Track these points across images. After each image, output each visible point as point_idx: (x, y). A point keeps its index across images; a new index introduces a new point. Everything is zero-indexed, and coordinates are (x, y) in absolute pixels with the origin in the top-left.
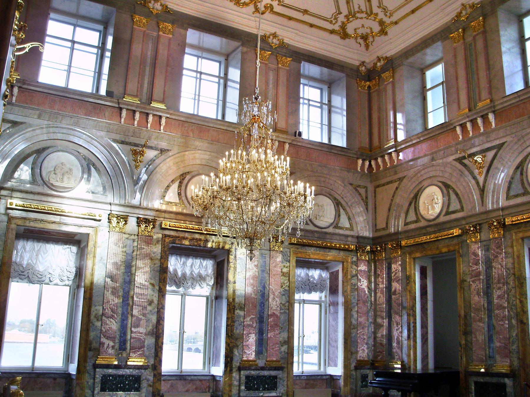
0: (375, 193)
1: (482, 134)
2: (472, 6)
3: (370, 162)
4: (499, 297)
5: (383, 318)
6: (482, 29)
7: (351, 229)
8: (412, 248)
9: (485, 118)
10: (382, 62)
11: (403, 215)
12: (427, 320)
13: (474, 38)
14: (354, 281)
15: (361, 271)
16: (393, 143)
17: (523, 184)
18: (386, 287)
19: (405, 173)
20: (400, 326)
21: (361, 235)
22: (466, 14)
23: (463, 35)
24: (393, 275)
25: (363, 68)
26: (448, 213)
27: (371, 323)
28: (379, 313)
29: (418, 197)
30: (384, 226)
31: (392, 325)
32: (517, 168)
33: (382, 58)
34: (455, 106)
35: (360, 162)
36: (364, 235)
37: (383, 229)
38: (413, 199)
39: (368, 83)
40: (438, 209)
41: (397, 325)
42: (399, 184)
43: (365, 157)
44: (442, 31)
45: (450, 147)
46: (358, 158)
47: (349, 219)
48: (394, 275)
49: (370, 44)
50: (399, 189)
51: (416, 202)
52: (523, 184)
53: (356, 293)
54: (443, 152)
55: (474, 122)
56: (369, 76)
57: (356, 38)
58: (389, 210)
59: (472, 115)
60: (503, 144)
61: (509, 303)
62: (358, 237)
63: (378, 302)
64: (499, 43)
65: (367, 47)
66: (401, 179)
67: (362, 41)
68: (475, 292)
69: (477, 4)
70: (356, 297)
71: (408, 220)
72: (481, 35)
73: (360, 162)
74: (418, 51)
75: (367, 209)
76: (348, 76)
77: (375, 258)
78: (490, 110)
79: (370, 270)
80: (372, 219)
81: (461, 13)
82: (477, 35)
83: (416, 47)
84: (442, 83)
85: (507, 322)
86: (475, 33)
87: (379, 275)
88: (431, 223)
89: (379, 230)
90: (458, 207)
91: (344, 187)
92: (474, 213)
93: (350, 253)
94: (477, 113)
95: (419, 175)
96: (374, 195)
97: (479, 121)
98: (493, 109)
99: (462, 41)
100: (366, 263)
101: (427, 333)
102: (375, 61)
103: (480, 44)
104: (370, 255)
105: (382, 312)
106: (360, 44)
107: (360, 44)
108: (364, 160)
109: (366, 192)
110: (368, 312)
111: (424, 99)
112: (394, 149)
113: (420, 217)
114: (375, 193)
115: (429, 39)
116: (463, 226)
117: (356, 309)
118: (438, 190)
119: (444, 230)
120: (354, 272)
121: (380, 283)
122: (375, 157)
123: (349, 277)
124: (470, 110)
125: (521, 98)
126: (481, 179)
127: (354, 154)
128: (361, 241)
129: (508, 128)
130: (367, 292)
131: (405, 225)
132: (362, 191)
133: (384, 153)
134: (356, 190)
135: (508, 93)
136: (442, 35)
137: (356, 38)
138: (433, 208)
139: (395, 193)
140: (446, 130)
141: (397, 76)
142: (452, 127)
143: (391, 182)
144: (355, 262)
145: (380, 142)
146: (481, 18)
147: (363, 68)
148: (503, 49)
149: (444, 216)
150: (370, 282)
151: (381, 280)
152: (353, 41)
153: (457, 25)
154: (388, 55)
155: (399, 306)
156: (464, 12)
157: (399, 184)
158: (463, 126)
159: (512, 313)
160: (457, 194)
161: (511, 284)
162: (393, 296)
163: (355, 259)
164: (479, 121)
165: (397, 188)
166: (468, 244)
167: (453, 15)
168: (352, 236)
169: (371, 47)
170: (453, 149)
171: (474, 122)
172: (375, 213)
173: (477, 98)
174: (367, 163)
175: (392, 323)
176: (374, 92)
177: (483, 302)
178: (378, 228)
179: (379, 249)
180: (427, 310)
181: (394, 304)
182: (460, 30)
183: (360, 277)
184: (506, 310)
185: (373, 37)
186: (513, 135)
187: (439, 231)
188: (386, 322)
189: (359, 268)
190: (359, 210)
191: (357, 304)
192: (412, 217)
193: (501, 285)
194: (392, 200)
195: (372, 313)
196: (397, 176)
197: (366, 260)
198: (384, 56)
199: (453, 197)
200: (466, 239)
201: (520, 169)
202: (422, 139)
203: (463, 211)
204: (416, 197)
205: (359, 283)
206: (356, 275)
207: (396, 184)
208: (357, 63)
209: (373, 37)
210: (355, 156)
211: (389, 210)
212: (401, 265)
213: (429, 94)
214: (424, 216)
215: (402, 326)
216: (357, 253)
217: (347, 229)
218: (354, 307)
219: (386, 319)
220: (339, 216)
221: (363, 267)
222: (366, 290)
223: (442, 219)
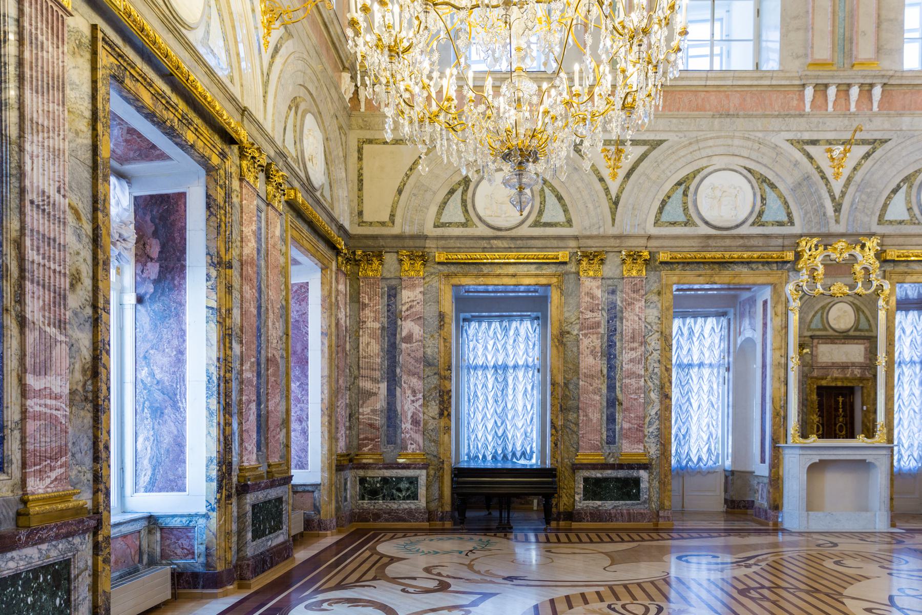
4: (631, 361)
18: (383, 328)
26: (536, 224)
48: (407, 310)
61: (646, 370)
68: (588, 351)
149: (530, 226)
159: (650, 384)
161: (653, 344)
177: (600, 365)
184: (643, 380)
193: (635, 345)
212: (423, 293)
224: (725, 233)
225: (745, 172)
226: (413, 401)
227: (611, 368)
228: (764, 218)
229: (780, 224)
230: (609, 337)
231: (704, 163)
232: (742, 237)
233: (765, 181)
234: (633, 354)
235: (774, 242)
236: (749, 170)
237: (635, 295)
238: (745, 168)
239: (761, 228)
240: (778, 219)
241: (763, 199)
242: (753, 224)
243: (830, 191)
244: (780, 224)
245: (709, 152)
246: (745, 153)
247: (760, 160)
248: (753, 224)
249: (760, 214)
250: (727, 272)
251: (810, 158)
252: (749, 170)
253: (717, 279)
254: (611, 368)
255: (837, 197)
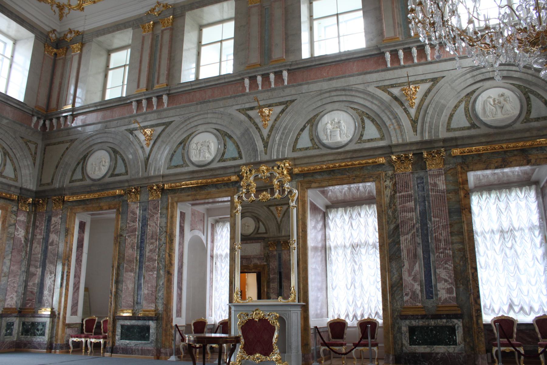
0: (45, 151)
1: (155, 112)
2: (166, 6)
3: (44, 121)
4: (151, 250)
5: (36, 267)
6: (170, 26)
7: (16, 179)
8: (74, 204)
9: (159, 98)
10: (73, 35)
11: (69, 173)
12: (80, 271)
13: (162, 31)
14: (11, 230)
15: (20, 221)
16: (71, 107)
17: (183, 157)
18: (43, 238)
19: (78, 136)
20: (53, 275)
21: (25, 187)
22: (159, 11)
23: (153, 28)
24: (52, 227)
25: (54, 35)
26: (112, 175)
27: (23, 272)
28: (32, 263)
29: (87, 159)
30: (50, 181)
31: (45, 274)
32: (181, 143)
33: (74, 31)
34: (135, 84)
35: (35, 119)
36: (28, 187)
37: (48, 184)
38: (82, 159)
39: (55, 50)
40: (104, 170)
41: (51, 273)
42: (70, 145)
43: (40, 116)
44: (135, 20)
45: (124, 118)
46: (33, 115)
47: (15, 170)
49: (64, 15)
50: (69, 150)
51: (84, 162)
52: (183, 157)
53: (12, 241)
54: (116, 122)
55: (149, 100)
56: (57, 44)
57: (52, 6)
58: (57, 167)
59: (148, 94)
60: (172, 122)
61: (159, 256)
62: (21, 189)
63: (33, 252)
64: (182, 40)
65: (61, 17)
66: (72, 141)
67: (57, 10)
68: (130, 246)
69: (170, 5)
70: (11, 246)
71: (74, 179)
72: (168, 31)
73: (35, 119)
74: (110, 32)
75: (34, 164)
76: (36, 38)
77: (35, 210)
78: (166, 93)
79: (28, 222)
80: (38, 174)
81: (154, 9)
82: (165, 29)
83: (108, 28)
84: (125, 66)
85: (156, 272)
86: (163, 28)
87: (37, 227)
88: (95, 183)
89: (44, 185)
90: (123, 171)
91: (14, 139)
92: (136, 177)
93: (11, 202)
94: (154, 93)
95: (91, 139)
96: (43, 152)
97: (154, 100)
98: (168, 92)
99: (151, 32)
100: (26, 214)
101: (79, 282)
102: (66, 33)
103: (167, 37)
104: (31, 206)
105: (36, 261)
106: (54, 11)
107: (54, 11)
108: (39, 118)
109: (36, 148)
110: (22, 261)
111: (106, 76)
112: (71, 113)
113: (86, 177)
114: (45, 151)
115: (122, 24)
116: (126, 188)
117: (10, 258)
118: (107, 155)
119: (107, 189)
120: (12, 222)
121: (38, 234)
122: (50, 118)
123: (7, 225)
124: (147, 90)
125: (193, 87)
126: (147, 150)
127: (30, 110)
128: (24, 194)
129: (178, 110)
130: (23, 242)
131: (70, 182)
132: (32, 147)
133: (60, 115)
134: (27, 144)
135: (182, 82)
136: (135, 23)
137: (52, 6)
138: (100, 169)
139: (65, 152)
140: (122, 103)
141: (85, 50)
142: (129, 101)
143: (63, 142)
144: (15, 211)
145: (57, 105)
146: (171, 17)
147: (54, 35)
148: (185, 47)
150: (27, 232)
151: (39, 231)
152: (48, 6)
153: (149, 18)
154: (81, 29)
155: (54, 255)
156: (157, 9)
157: (70, 145)
158: (139, 102)
159: (160, 265)
160: (123, 160)
161: (163, 240)
162: (50, 247)
163: (15, 209)
164: (154, 100)
165: (67, 149)
166: (128, 204)
167: (148, 9)
168: (16, 187)
169: (64, 18)
170: (127, 120)
171: (149, 100)
172: (42, 169)
173: (156, 81)
174: (41, 122)
175: (46, 272)
176: (60, 59)
177: (136, 254)
178: (43, 182)
179: (41, 202)
180: (81, 261)
181: (49, 254)
182: (152, 22)
183: (17, 227)
184: (156, 262)
185: (70, 9)
186: (181, 117)
187: (103, 190)
188: (39, 271)
189: (18, 218)
190: (26, 164)
191: (12, 252)
192: (78, 175)
193: (154, 241)
194: (61, 159)
195: (25, 263)
196: (70, 138)
197: (27, 211)
198: (76, 30)
199: (120, 161)
200: (126, 199)
201: (182, 145)
202: (99, 108)
203: (127, 174)
204: (85, 158)
205: (16, 233)
206: (15, 225)
207: (67, 145)
208: (48, 29)
209: (70, 9)
210: (31, 113)
211: (57, 167)
212: (61, 218)
213: (110, 73)
214: (90, 176)
215: (55, 275)
216: (18, 203)
217: (11, 179)
218: (8, 255)
219: (39, 268)
220: (5, 165)
221: (22, 218)
222: (23, 240)
223: (107, 180)
224: (203, 168)
225: (215, 131)
226: (50, 278)
227: (141, 255)
228: (225, 157)
229: (234, 159)
230: (141, 236)
231: (194, 130)
232: (212, 170)
233: (226, 135)
234: (151, 247)
235: (229, 171)
236: (217, 130)
237: (154, 211)
238: (215, 129)
239: (223, 163)
240: (233, 156)
241: (225, 145)
242: (219, 161)
243: (261, 136)
244: (234, 159)
245: (196, 123)
246: (214, 121)
247: (222, 123)
248: (219, 161)
249: (223, 154)
250: (203, 192)
251: (250, 118)
252: (217, 130)
253: (198, 197)
254: (141, 255)
255: (265, 139)
